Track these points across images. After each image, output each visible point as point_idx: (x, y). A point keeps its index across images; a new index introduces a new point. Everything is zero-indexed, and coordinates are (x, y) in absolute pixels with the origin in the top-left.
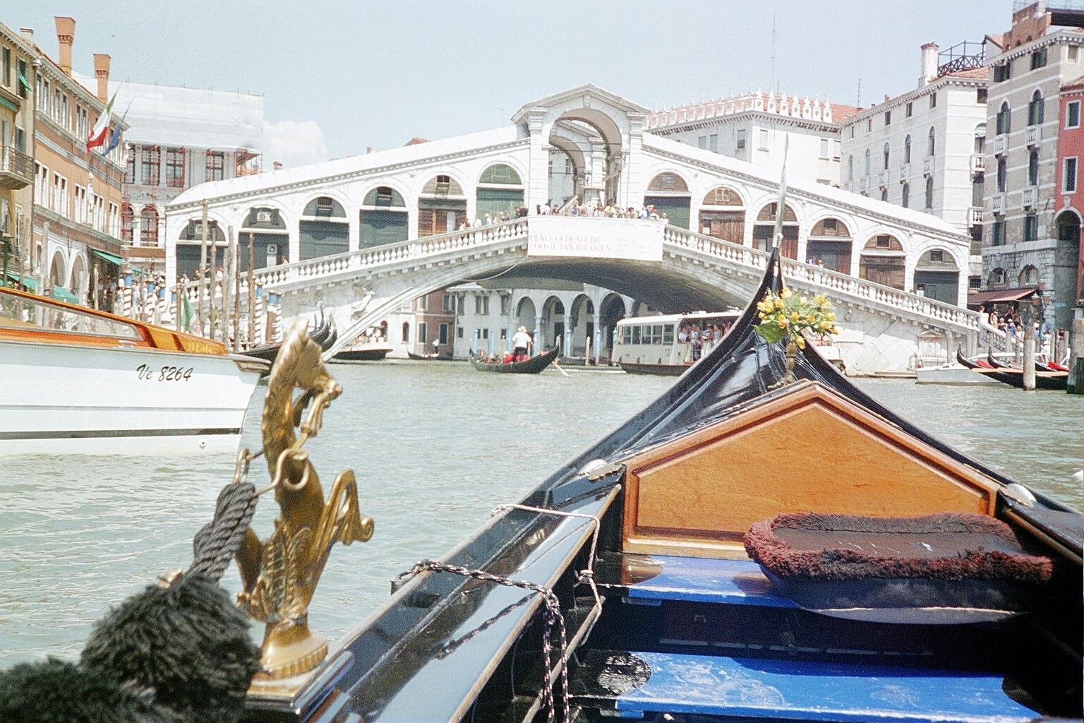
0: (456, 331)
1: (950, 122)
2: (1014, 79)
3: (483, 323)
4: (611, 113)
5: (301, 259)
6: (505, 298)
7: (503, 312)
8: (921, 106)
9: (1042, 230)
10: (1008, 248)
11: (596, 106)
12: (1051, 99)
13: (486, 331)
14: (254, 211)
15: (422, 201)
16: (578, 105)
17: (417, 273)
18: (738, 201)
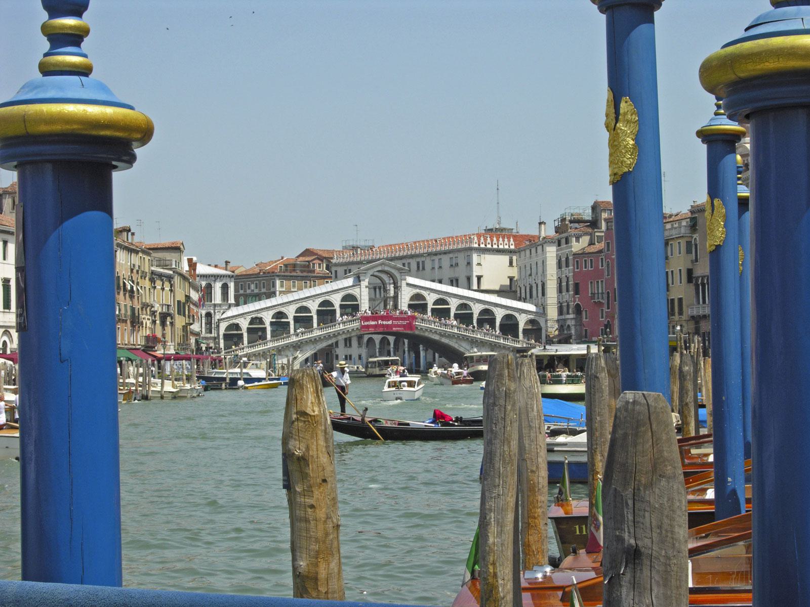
0: (334, 356)
1: (548, 259)
2: (562, 247)
3: (349, 351)
4: (393, 271)
5: (272, 336)
6: (360, 338)
7: (359, 344)
8: (540, 248)
9: (571, 311)
10: (563, 317)
11: (386, 268)
12: (571, 257)
13: (350, 356)
17: (318, 341)
18: (448, 304)
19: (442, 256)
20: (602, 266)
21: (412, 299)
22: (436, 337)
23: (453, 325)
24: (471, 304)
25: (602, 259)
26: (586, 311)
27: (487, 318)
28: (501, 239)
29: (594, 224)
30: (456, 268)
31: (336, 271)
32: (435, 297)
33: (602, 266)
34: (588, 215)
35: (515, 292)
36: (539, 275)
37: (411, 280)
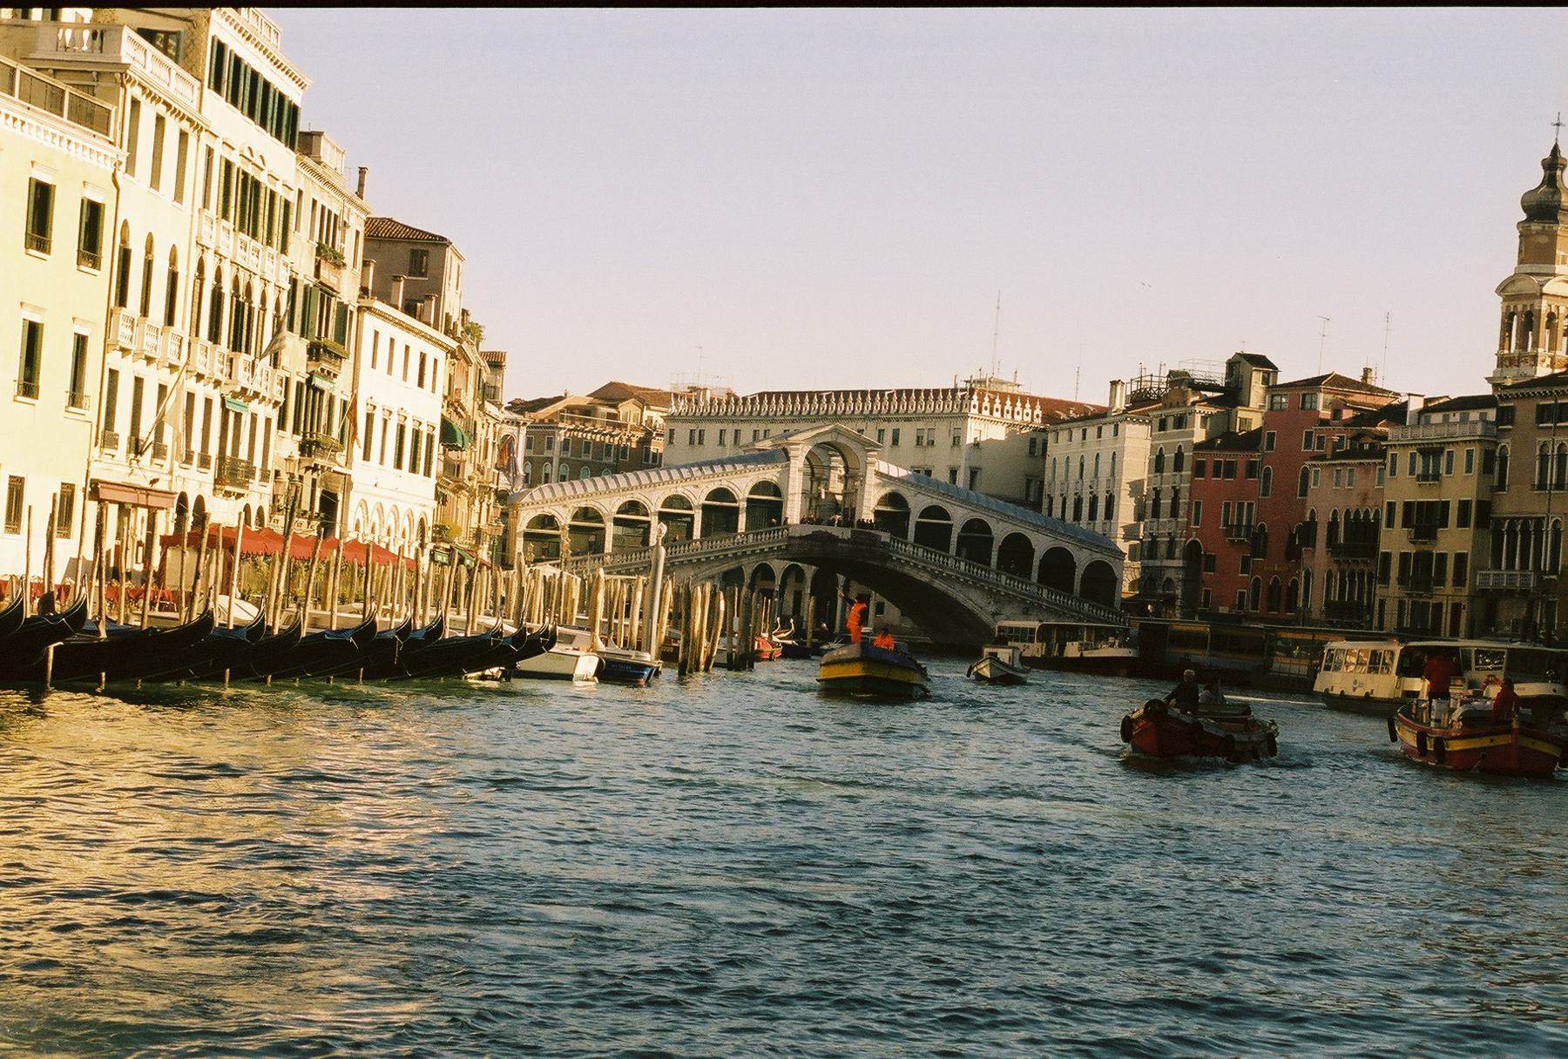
4: (852, 445)
8: (1108, 431)
9: (1178, 552)
10: (1158, 563)
11: (842, 440)
12: (1188, 454)
15: (705, 507)
16: (828, 439)
19: (902, 426)
24: (992, 523)
27: (1017, 548)
29: (1232, 394)
30: (930, 450)
31: (672, 431)
34: (1219, 375)
35: (1037, 506)
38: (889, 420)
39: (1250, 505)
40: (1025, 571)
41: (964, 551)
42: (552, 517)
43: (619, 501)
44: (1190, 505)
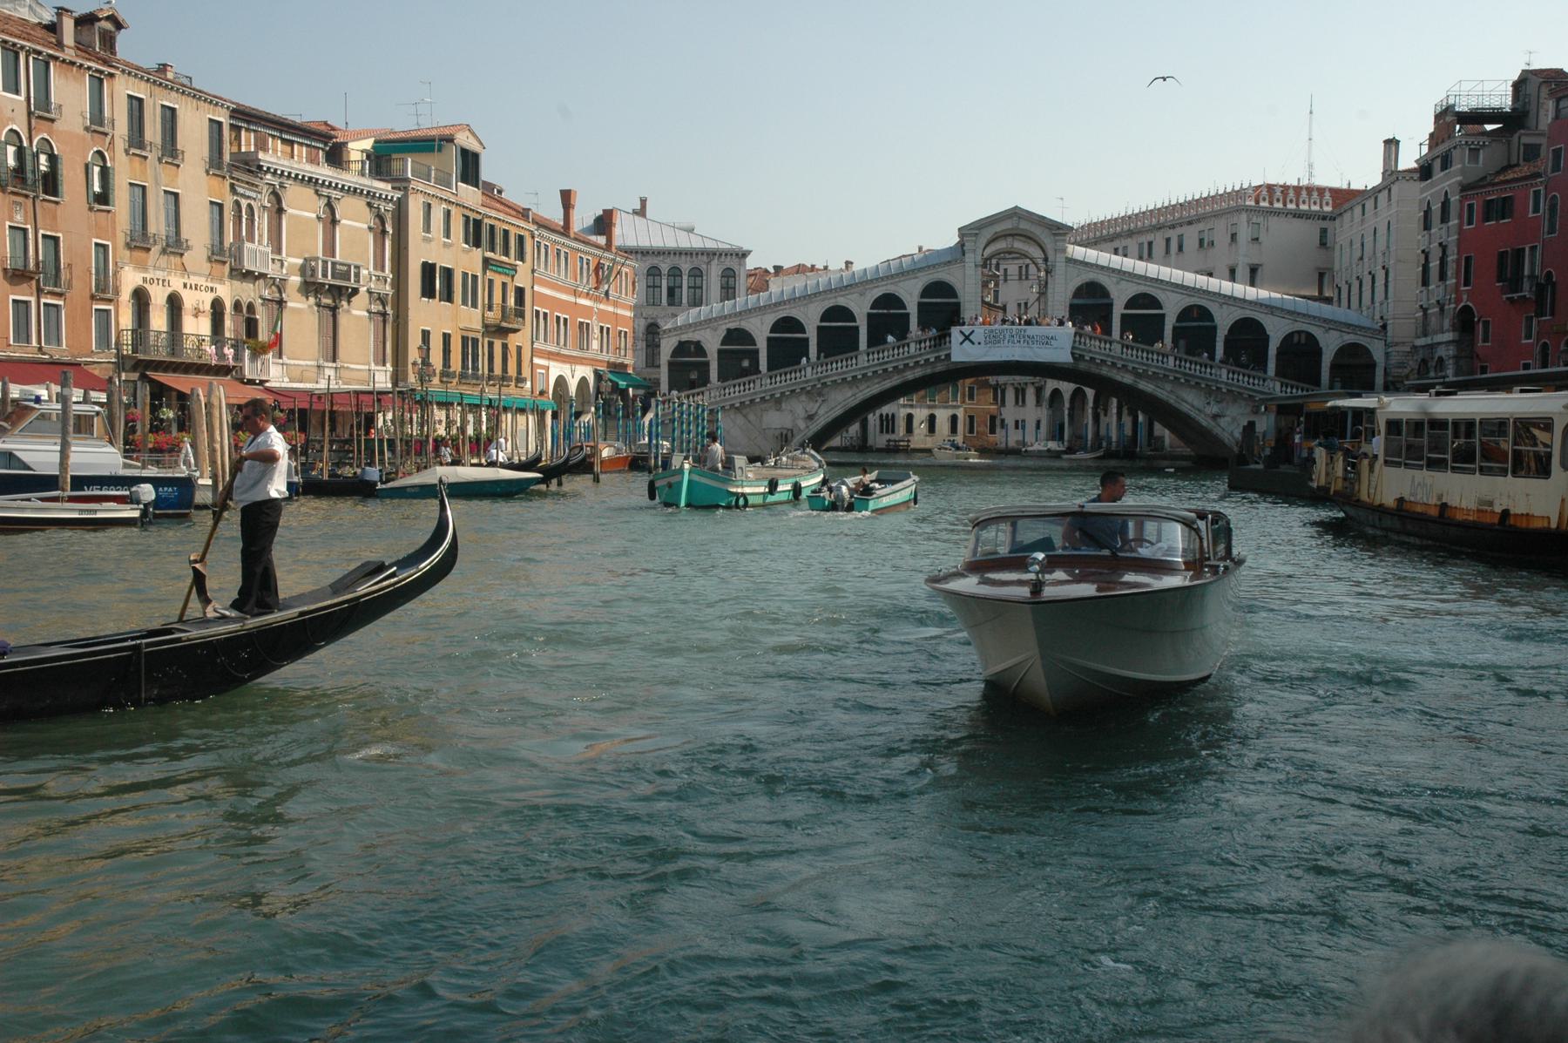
4: (1039, 232)
6: (1039, 391)
7: (1038, 402)
8: (1383, 196)
10: (1428, 340)
11: (1024, 225)
12: (1454, 198)
14: (729, 330)
16: (1006, 226)
20: (1536, 209)
21: (1078, 293)
22: (1128, 379)
23: (1165, 353)
24: (1213, 308)
25: (1537, 193)
26: (1486, 324)
28: (1304, 193)
29: (1513, 120)
32: (1132, 290)
33: (1536, 209)
34: (1501, 98)
36: (1379, 255)
37: (1078, 252)
38: (1173, 227)
39: (1533, 249)
40: (1261, 362)
41: (1182, 343)
42: (698, 344)
43: (771, 319)
44: (1458, 262)
